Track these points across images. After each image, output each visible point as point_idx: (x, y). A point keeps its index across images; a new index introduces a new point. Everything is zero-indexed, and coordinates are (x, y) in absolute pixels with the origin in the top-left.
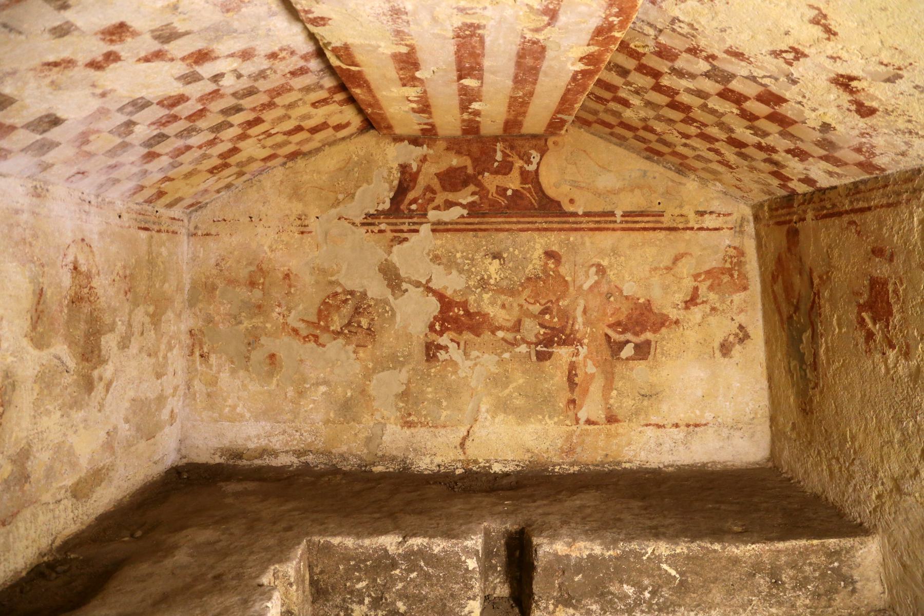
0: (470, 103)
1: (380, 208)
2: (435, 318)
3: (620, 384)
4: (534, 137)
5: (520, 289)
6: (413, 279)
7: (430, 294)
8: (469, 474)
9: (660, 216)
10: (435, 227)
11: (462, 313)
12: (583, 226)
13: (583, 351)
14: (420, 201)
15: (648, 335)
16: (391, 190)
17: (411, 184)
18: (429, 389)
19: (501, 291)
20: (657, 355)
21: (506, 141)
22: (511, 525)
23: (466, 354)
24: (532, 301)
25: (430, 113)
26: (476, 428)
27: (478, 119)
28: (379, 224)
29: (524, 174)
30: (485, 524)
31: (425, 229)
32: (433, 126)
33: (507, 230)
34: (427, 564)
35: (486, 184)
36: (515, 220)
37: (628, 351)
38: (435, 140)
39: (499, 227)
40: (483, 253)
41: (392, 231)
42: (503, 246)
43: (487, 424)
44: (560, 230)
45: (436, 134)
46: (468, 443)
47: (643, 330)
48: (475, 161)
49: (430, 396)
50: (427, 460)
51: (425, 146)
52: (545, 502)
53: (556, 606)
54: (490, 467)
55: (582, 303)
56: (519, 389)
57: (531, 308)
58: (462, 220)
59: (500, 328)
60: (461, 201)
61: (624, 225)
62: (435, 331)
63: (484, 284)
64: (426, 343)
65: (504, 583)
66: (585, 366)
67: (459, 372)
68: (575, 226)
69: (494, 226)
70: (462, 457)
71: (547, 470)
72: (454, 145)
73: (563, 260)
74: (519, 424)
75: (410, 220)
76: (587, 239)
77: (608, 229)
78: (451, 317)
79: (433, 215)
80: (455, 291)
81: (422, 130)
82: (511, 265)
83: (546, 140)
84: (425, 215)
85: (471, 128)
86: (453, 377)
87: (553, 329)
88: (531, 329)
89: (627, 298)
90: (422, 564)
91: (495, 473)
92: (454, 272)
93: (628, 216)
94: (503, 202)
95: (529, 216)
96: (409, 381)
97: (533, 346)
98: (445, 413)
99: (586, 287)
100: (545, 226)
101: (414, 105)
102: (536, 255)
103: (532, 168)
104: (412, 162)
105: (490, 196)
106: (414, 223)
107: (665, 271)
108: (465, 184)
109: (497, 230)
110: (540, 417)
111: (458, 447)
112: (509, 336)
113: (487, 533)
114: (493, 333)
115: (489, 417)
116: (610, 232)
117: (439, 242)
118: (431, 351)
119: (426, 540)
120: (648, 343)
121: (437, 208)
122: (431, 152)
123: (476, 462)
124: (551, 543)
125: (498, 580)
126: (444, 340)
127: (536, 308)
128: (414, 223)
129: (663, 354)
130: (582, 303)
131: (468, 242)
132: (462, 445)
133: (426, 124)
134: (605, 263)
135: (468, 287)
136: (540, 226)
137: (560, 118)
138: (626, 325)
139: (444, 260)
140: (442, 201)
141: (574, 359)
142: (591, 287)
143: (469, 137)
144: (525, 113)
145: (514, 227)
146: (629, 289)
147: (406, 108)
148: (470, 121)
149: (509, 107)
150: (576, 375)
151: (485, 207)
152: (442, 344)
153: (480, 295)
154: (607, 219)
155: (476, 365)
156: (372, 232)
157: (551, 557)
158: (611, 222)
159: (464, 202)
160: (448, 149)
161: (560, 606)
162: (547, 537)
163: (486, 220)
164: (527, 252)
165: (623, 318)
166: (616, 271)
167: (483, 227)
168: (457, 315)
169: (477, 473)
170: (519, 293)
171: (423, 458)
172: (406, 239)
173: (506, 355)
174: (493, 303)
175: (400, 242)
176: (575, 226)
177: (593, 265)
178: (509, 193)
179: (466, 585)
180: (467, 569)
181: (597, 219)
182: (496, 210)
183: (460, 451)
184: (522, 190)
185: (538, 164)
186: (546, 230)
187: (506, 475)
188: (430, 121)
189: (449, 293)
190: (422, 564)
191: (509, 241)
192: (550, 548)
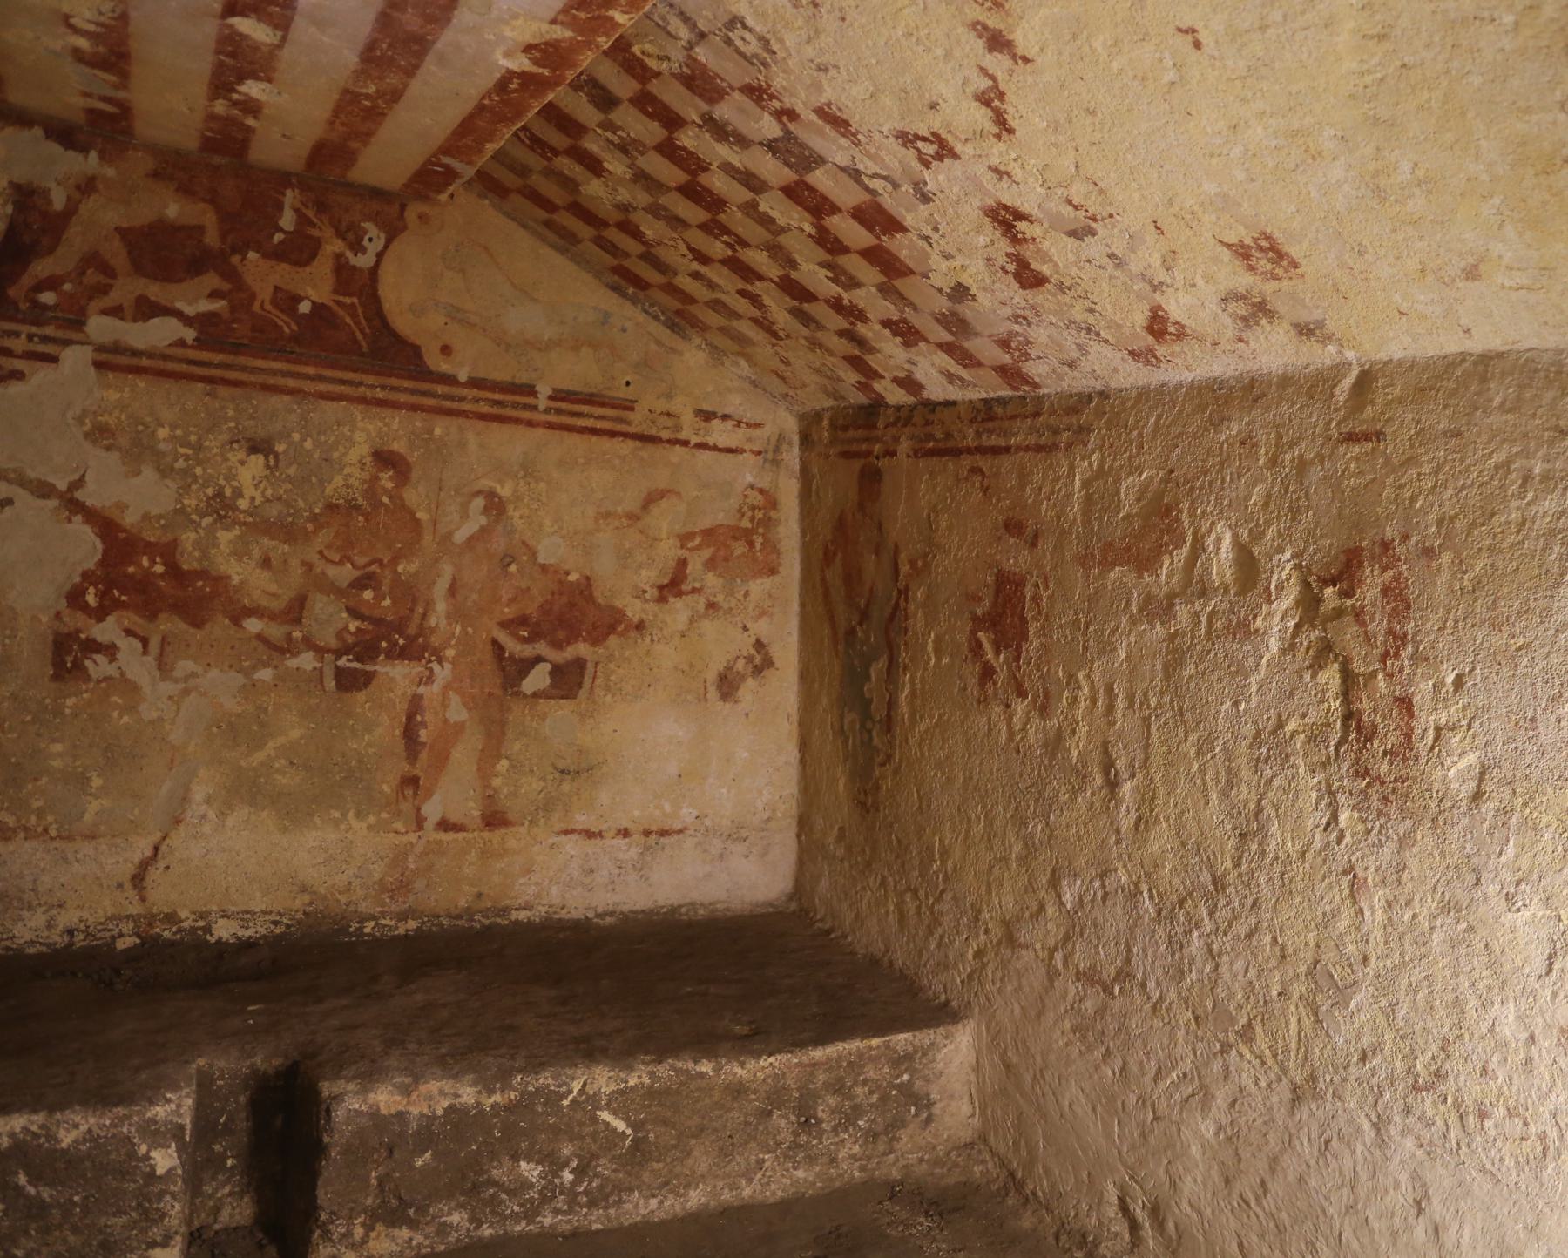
0: (241, 79)
2: (86, 575)
3: (517, 746)
4: (377, 193)
5: (310, 527)
6: (32, 474)
7: (78, 518)
8: (150, 947)
9: (626, 408)
10: (104, 357)
11: (159, 569)
12: (466, 407)
13: (443, 673)
14: (67, 287)
15: (582, 649)
18: (58, 748)
19: (265, 527)
20: (597, 690)
22: (264, 1059)
23: (163, 668)
24: (336, 557)
25: (124, 76)
26: (177, 839)
27: (250, 122)
29: (342, 270)
30: (201, 1062)
31: (76, 358)
32: (125, 110)
33: (291, 392)
34: (35, 1179)
35: (249, 279)
36: (311, 370)
37: (538, 679)
39: (271, 381)
40: (225, 437)
43: (207, 829)
44: (414, 408)
45: (128, 132)
46: (154, 875)
47: (573, 637)
49: (57, 763)
50: (38, 919)
51: (93, 154)
52: (344, 1002)
53: (368, 1228)
54: (207, 929)
55: (447, 570)
57: (332, 571)
58: (179, 352)
60: (179, 305)
61: (552, 418)
62: (85, 607)
63: (221, 507)
64: (57, 634)
65: (241, 1194)
66: (445, 705)
67: (143, 707)
68: (447, 404)
69: (260, 378)
70: (135, 909)
71: (344, 930)
72: (172, 168)
73: (415, 475)
74: (284, 830)
75: (34, 329)
76: (471, 438)
77: (517, 421)
78: (132, 577)
79: (99, 327)
80: (146, 517)
81: (91, 111)
82: (292, 471)
83: (403, 207)
84: (79, 324)
85: (228, 140)
86: (126, 719)
87: (378, 622)
88: (330, 619)
89: (544, 568)
90: (22, 1179)
91: (219, 941)
92: (149, 473)
93: (563, 400)
94: (288, 327)
95: (346, 368)
97: (329, 657)
98: (94, 806)
99: (460, 536)
100: (380, 394)
102: (352, 457)
103: (364, 261)
104: (53, 185)
105: (256, 307)
106: (45, 339)
107: (625, 522)
109: (266, 388)
110: (337, 814)
111: (128, 885)
112: (276, 632)
113: (204, 1085)
114: (236, 621)
115: (212, 815)
116: (521, 429)
117: (113, 395)
118: (68, 655)
119: (40, 1118)
120: (579, 664)
121: (115, 312)
122: (110, 172)
123: (171, 918)
124: (365, 1091)
125: (227, 1189)
126: (107, 630)
127: (343, 574)
128: (45, 339)
129: (608, 688)
130: (447, 570)
131: (189, 405)
132: (138, 879)
134: (505, 491)
135: (182, 511)
136: (369, 393)
137: (448, 168)
138: (537, 624)
139: (124, 441)
141: (422, 690)
142: (471, 539)
143: (217, 160)
144: (369, 134)
145: (308, 386)
146: (550, 550)
148: (229, 121)
149: (337, 111)
150: (424, 724)
152: (99, 639)
153: (211, 530)
154: (518, 398)
157: (363, 1121)
158: (526, 407)
159: (190, 310)
160: (156, 175)
161: (380, 1227)
162: (354, 1078)
165: (532, 609)
166: (527, 511)
168: (148, 574)
169: (172, 943)
171: (26, 914)
172: (18, 375)
173: (265, 674)
174: (239, 554)
176: (447, 404)
177: (479, 493)
178: (304, 307)
179: (145, 1213)
180: (151, 1176)
181: (497, 396)
183: (131, 893)
184: (335, 307)
185: (380, 256)
186: (381, 403)
187: (247, 945)
188: (121, 94)
189: (130, 519)
190: (22, 1179)
192: (361, 1102)
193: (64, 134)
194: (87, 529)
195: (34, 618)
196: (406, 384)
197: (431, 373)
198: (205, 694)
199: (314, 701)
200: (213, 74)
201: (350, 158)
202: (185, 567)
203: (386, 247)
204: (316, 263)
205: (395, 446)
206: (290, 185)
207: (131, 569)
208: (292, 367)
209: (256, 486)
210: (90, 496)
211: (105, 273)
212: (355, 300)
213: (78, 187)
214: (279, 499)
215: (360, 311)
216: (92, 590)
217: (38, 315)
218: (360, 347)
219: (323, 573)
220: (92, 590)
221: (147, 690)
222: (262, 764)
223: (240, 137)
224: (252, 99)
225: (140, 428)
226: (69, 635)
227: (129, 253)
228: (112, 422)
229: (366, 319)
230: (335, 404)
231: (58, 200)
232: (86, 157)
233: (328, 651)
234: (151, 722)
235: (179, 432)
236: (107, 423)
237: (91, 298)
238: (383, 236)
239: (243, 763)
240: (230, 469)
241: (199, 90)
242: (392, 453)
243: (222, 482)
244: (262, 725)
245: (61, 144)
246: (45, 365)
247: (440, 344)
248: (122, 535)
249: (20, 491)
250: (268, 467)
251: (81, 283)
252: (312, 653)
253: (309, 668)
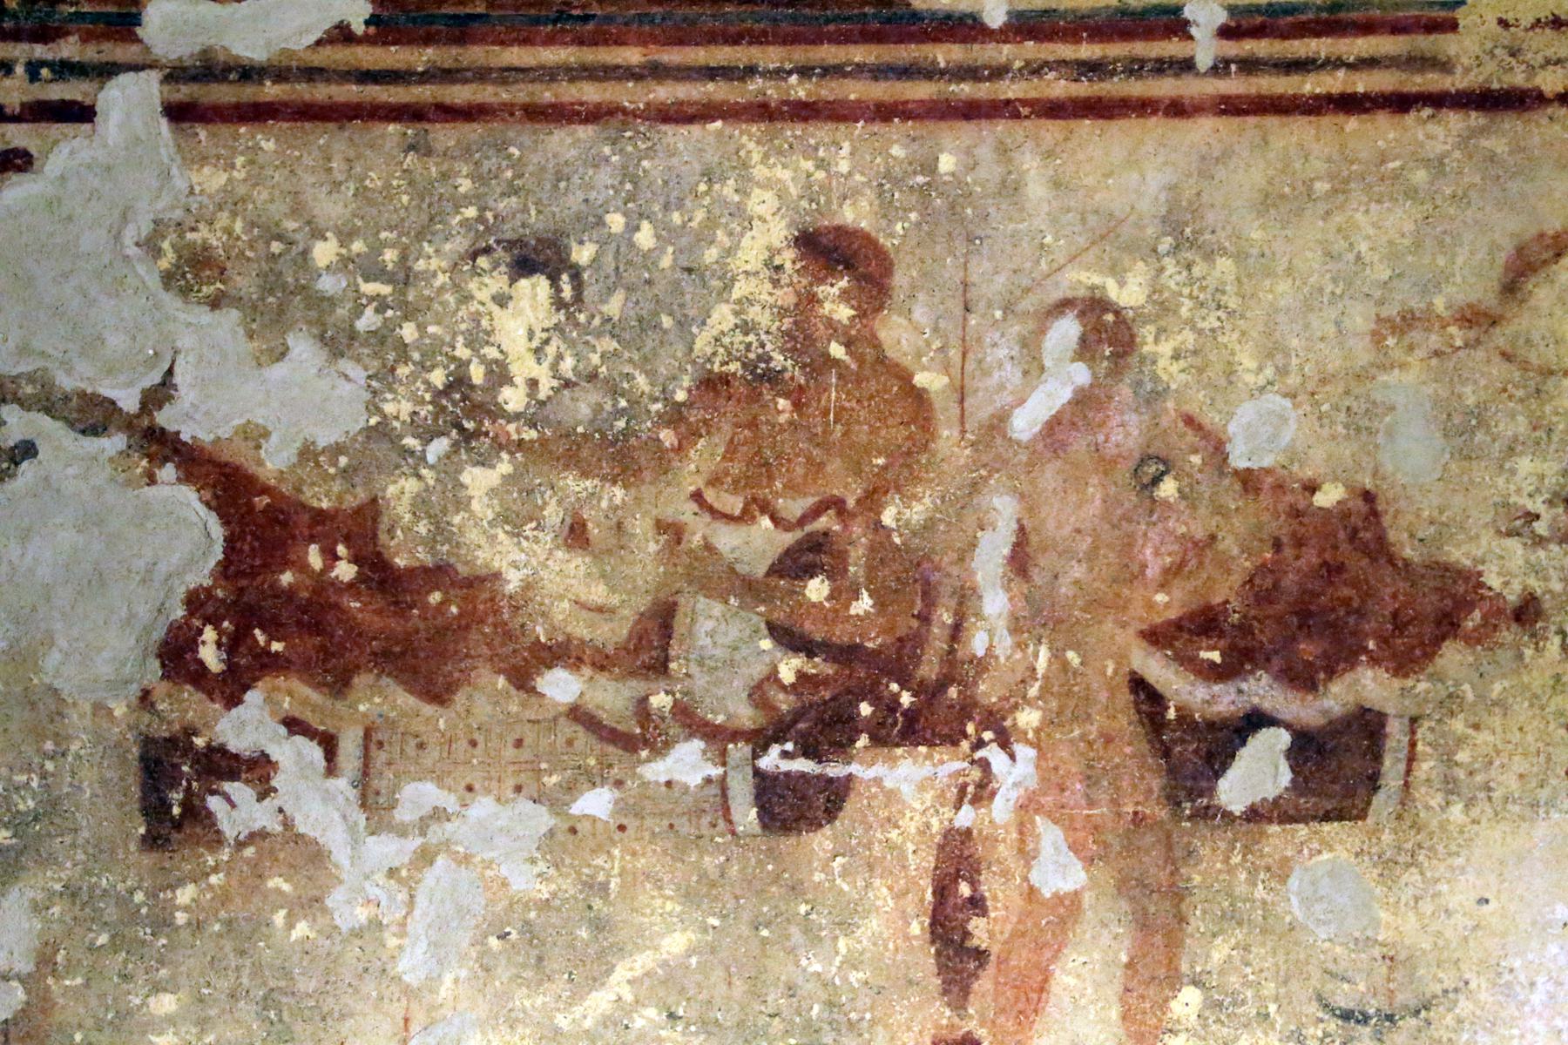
2: (196, 601)
3: (1220, 952)
5: (667, 437)
7: (168, 472)
9: (1433, 27)
10: (184, 92)
11: (345, 571)
12: (1010, 90)
13: (1014, 772)
15: (1368, 685)
18: (166, 1004)
20: (1420, 792)
23: (372, 801)
24: (735, 504)
31: (128, 103)
33: (594, 115)
36: (632, 56)
37: (1257, 772)
39: (547, 96)
40: (459, 244)
42: (574, 201)
44: (885, 112)
47: (1341, 658)
55: (1003, 509)
56: (666, 984)
57: (728, 539)
59: (560, 653)
61: (1234, 85)
62: (198, 676)
63: (466, 412)
64: (147, 741)
66: (1027, 855)
67: (335, 899)
68: (965, 90)
69: (520, 93)
73: (900, 280)
75: (39, 51)
76: (1030, 163)
77: (1144, 107)
78: (290, 594)
80: (308, 453)
82: (614, 306)
86: (302, 929)
87: (846, 654)
88: (732, 657)
89: (1248, 481)
92: (303, 348)
93: (1257, 32)
95: (711, 38)
96: (45, 960)
97: (739, 751)
99: (1026, 423)
100: (799, 89)
102: (751, 253)
106: (65, 69)
107: (1457, 334)
109: (537, 114)
112: (611, 697)
114: (522, 679)
116: (1156, 126)
117: (212, 179)
118: (174, 787)
120: (1366, 726)
126: (246, 725)
127: (756, 544)
128: (65, 69)
129: (1450, 787)
130: (1003, 509)
131: (374, 181)
134: (1129, 293)
135: (382, 432)
136: (773, 92)
138: (1244, 629)
139: (245, 283)
141: (966, 817)
142: (1053, 425)
145: (628, 95)
146: (1259, 431)
150: (977, 904)
152: (234, 746)
153: (449, 469)
154: (1140, 48)
155: (425, 857)
158: (1162, 67)
163: (475, 54)
164: (704, 237)
165: (1226, 591)
166: (1188, 338)
167: (460, 94)
168: (323, 584)
170: (663, 461)
173: (596, 803)
174: (516, 518)
176: (965, 90)
177: (1064, 305)
181: (1088, 51)
186: (805, 112)
189: (274, 462)
191: (605, 177)
194: (189, 496)
195: (99, 708)
196: (860, 54)
197: (916, 16)
198: (466, 859)
199: (711, 862)
202: (400, 562)
207: (287, 578)
209: (538, 352)
210: (186, 419)
214: (593, 377)
216: (209, 634)
219: (708, 547)
220: (209, 634)
221: (341, 854)
222: (606, 1021)
225: (276, 247)
226: (172, 741)
230: (695, 130)
233: (736, 735)
234: (357, 933)
235: (358, 246)
236: (206, 247)
239: (562, 1021)
240: (476, 318)
242: (841, 231)
243: (462, 352)
244: (599, 926)
248: (262, 501)
249: (45, 421)
250: (559, 304)
252: (697, 744)
253: (694, 780)
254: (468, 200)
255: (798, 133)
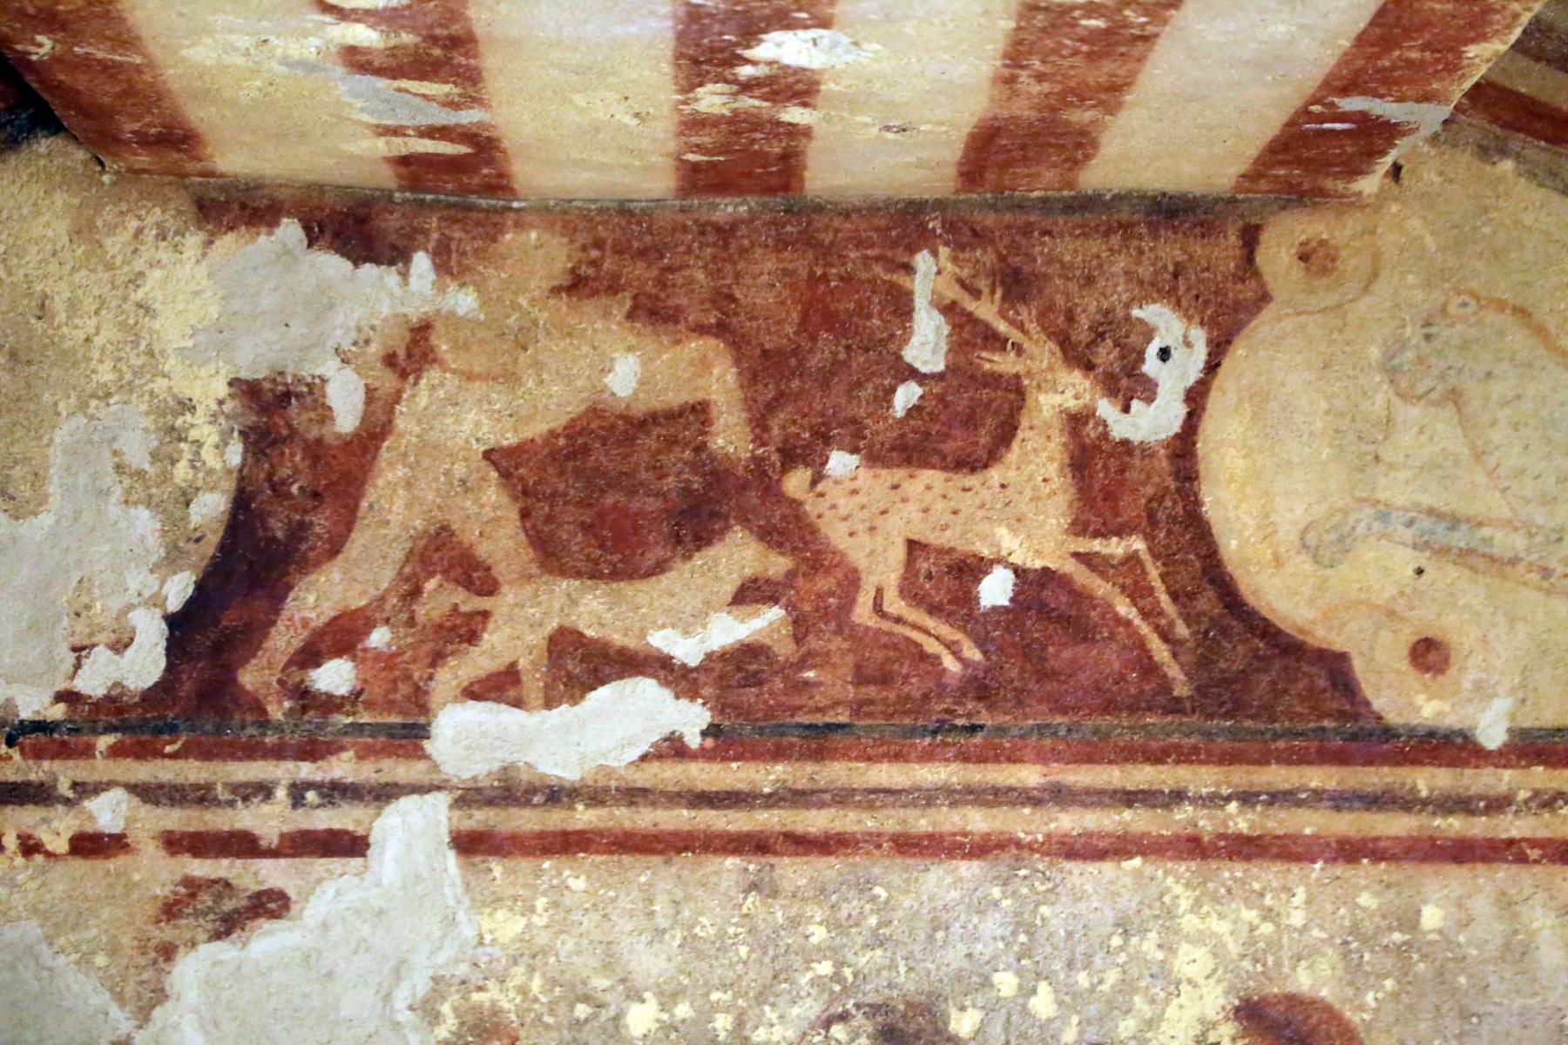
0: (751, 32)
1: (93, 681)
4: (1171, 212)
10: (479, 818)
12: (1512, 826)
14: (379, 638)
16: (172, 560)
17: (321, 522)
21: (979, 236)
25: (470, 78)
27: (794, 114)
28: (84, 790)
29: (1094, 462)
31: (410, 832)
32: (484, 146)
33: (982, 848)
35: (836, 534)
36: (1029, 775)
38: (491, 225)
39: (922, 823)
40: (811, 1008)
41: (174, 843)
42: (954, 957)
44: (1350, 851)
45: (500, 186)
48: (768, 371)
51: (421, 262)
58: (671, 774)
60: (664, 640)
68: (1454, 825)
69: (889, 821)
72: (621, 261)
75: (306, 770)
79: (466, 737)
81: (404, 161)
83: (1250, 238)
84: (409, 736)
85: (747, 165)
94: (955, 654)
95: (1129, 755)
100: (1240, 821)
101: (363, 35)
103: (1150, 422)
104: (329, 367)
105: (862, 613)
106: (335, 792)
108: (695, 523)
117: (507, 926)
121: (500, 687)
122: (464, 301)
128: (335, 792)
131: (706, 928)
133: (431, 132)
136: (1206, 823)
137: (1363, 118)
140: (537, 639)
143: (728, 208)
144: (1116, 88)
145: (1024, 823)
147: (309, 48)
148: (736, 124)
149: (1016, 55)
151: (831, 686)
156: (30, 847)
159: (687, 650)
160: (576, 285)
163: (836, 772)
164: (1118, 1003)
167: (815, 821)
172: (270, 905)
175: (228, 926)
176: (1454, 825)
178: (995, 590)
182: (904, 708)
184: (1082, 576)
185: (1196, 398)
186: (1246, 848)
188: (469, 117)
193: (352, 226)
196: (1317, 777)
197: (1389, 733)
200: (681, 37)
201: (1082, 145)
203: (1212, 367)
204: (1014, 453)
205: (1303, 981)
206: (923, 239)
208: (978, 775)
211: (468, 585)
212: (1138, 544)
213: (390, 360)
215: (1154, 573)
217: (313, 726)
218: (1166, 686)
223: (776, 149)
224: (785, 68)
225: (582, 1011)
227: (525, 514)
228: (506, 1001)
229: (1175, 597)
230: (1108, 867)
231: (346, 411)
232: (404, 275)
235: (683, 1010)
236: (496, 1011)
237: (437, 658)
238: (1199, 336)
241: (653, 77)
242: (1293, 1000)
245: (345, 254)
246: (336, 864)
247: (1408, 636)
251: (411, 622)
254: (821, 952)
255: (1239, 874)
